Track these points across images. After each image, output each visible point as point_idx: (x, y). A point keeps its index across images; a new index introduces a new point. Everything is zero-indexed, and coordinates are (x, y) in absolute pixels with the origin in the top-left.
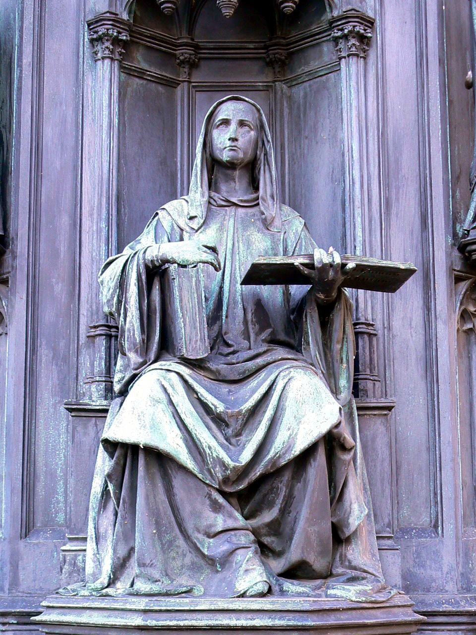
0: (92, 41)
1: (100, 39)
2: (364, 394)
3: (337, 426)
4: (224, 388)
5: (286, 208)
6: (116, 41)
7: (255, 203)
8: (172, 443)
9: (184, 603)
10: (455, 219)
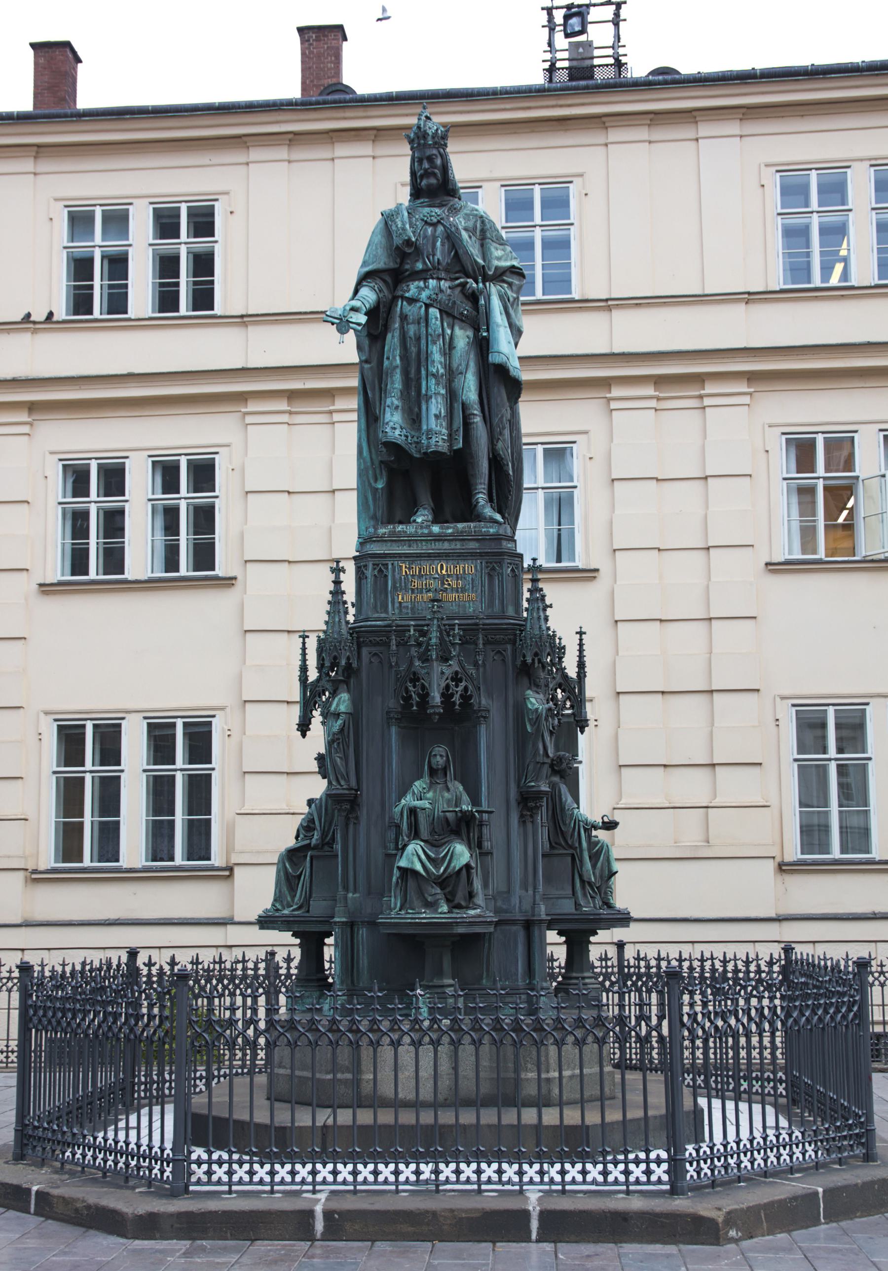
1: (391, 718)
4: (434, 849)
5: (456, 783)
6: (396, 719)
7: (446, 782)
8: (418, 867)
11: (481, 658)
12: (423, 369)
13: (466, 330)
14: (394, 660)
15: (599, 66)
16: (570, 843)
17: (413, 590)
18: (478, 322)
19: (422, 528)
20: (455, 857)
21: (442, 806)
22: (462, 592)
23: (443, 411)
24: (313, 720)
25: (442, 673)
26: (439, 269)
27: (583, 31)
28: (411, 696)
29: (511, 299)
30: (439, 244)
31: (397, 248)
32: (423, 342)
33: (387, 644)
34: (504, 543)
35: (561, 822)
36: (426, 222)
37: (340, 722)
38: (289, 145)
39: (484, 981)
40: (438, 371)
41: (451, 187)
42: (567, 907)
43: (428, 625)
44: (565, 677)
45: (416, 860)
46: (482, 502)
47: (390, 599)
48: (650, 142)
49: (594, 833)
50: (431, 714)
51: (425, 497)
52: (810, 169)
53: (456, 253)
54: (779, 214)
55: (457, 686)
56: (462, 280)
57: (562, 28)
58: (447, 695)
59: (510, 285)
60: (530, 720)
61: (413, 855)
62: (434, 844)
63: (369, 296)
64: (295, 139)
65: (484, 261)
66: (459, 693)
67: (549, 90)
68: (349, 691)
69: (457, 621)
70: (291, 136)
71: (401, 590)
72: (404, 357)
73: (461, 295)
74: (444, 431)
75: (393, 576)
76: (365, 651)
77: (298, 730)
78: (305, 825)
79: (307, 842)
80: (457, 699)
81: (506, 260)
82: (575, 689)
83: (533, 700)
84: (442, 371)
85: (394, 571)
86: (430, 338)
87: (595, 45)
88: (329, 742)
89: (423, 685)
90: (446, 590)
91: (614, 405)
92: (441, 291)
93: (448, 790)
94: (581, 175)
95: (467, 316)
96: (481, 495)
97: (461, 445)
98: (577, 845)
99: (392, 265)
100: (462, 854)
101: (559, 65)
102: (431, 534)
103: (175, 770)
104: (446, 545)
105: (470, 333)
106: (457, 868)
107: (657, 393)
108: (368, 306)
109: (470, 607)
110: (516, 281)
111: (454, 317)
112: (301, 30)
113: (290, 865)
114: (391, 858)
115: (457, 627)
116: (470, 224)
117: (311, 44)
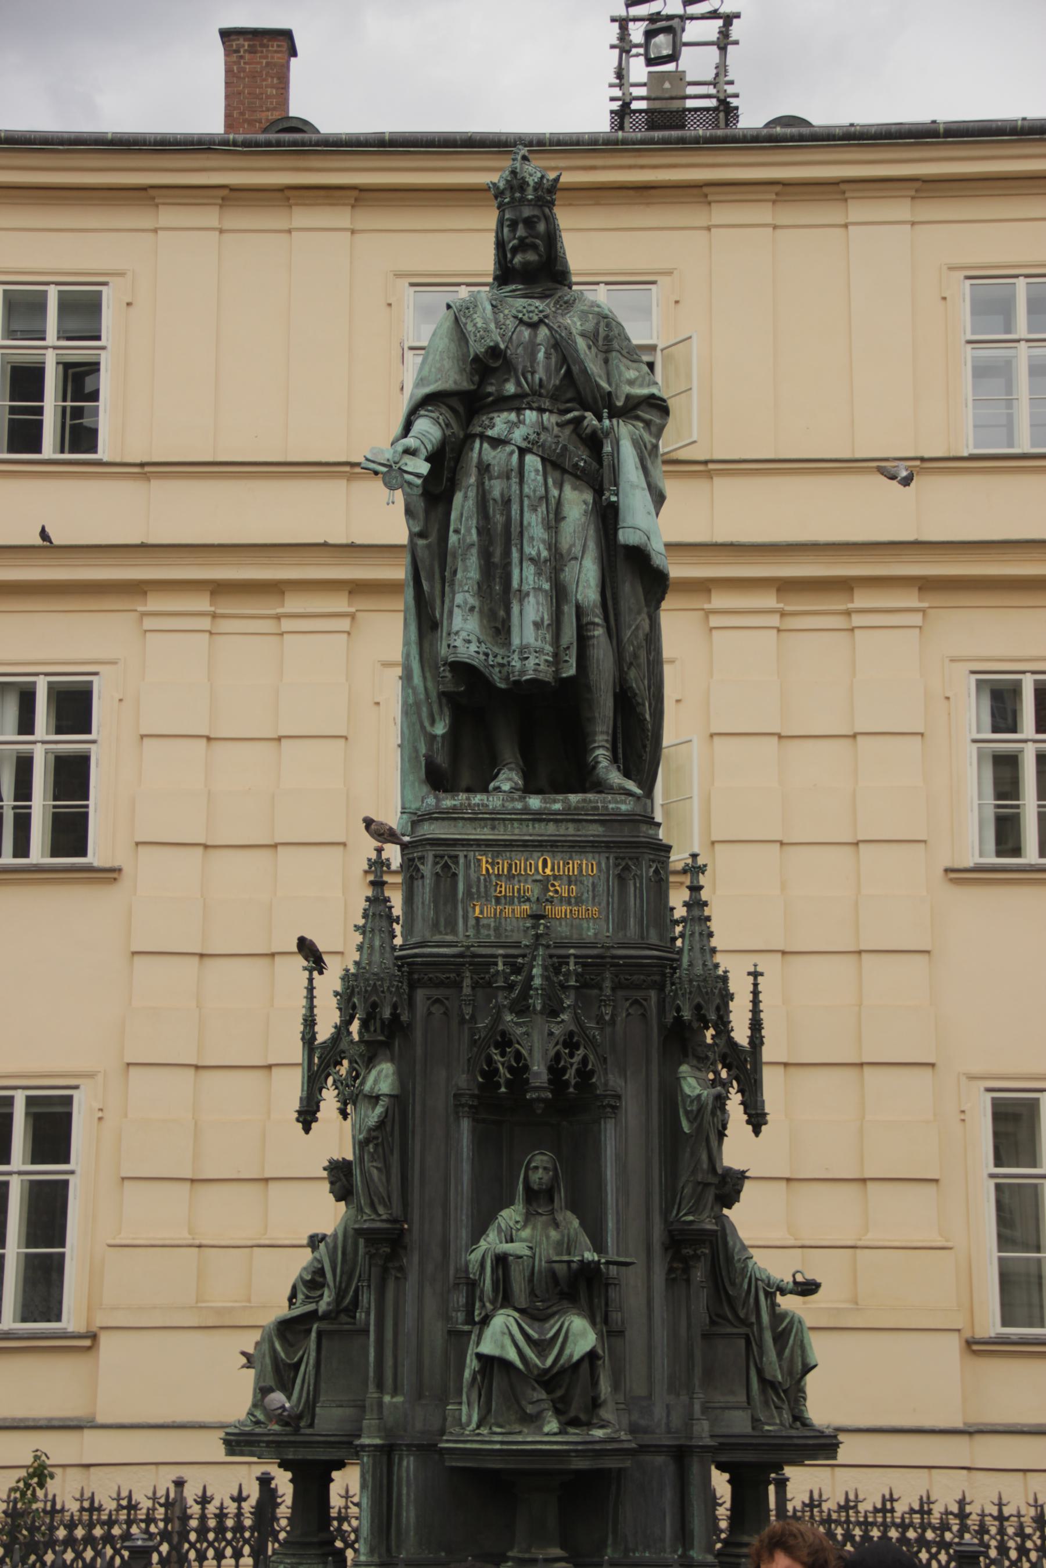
0: (456, 1106)
1: (463, 1105)
2: (610, 1330)
3: (594, 1347)
4: (536, 1325)
5: (569, 1214)
6: (471, 1107)
7: (552, 1212)
8: (512, 1355)
9: (520, 1438)
10: (665, 1213)
11: (609, 1010)
12: (514, 550)
13: (581, 491)
14: (468, 1011)
15: (696, 110)
16: (742, 1315)
17: (498, 900)
18: (599, 478)
19: (513, 800)
20: (571, 1339)
21: (547, 1252)
22: (577, 904)
23: (546, 617)
24: (322, 1104)
25: (551, 1034)
26: (541, 395)
27: (673, 57)
28: (497, 1070)
29: (649, 446)
30: (541, 355)
31: (476, 359)
32: (515, 508)
33: (458, 985)
34: (644, 828)
35: (726, 1280)
36: (521, 321)
37: (379, 1110)
38: (221, 206)
39: (609, 1551)
40: (539, 554)
41: (559, 268)
42: (739, 1423)
43: (524, 956)
44: (732, 1044)
45: (508, 1342)
46: (604, 763)
47: (461, 913)
48: (775, 227)
49: (779, 1299)
50: (532, 1100)
51: (508, 751)
52: (1017, 276)
53: (569, 371)
54: (969, 342)
55: (571, 1055)
56: (576, 413)
57: (641, 51)
58: (556, 1071)
59: (648, 424)
60: (687, 1113)
61: (503, 1333)
62: (533, 1314)
63: (428, 429)
64: (232, 196)
65: (610, 384)
66: (575, 1067)
67: (624, 142)
68: (392, 1060)
69: (572, 951)
70: (226, 192)
71: (479, 898)
72: (484, 530)
73: (574, 436)
74: (548, 648)
75: (467, 876)
76: (420, 994)
77: (298, 1120)
78: (308, 1277)
79: (311, 1307)
80: (570, 1075)
81: (641, 386)
82: (745, 1067)
83: (692, 1081)
84: (545, 554)
85: (467, 866)
86: (526, 502)
87: (689, 78)
88: (360, 1143)
89: (518, 1056)
90: (550, 901)
91: (715, 621)
92: (545, 428)
93: (557, 1226)
94: (669, 273)
95: (583, 470)
96: (601, 751)
97: (572, 671)
98: (753, 1319)
99: (465, 385)
100: (581, 1335)
101: (636, 105)
102: (526, 810)
103: (10, 1173)
104: (551, 829)
105: (589, 496)
106: (576, 1358)
107: (781, 605)
108: (429, 447)
109: (588, 929)
110: (654, 417)
111: (564, 471)
112: (226, 35)
113: (282, 1346)
114: (458, 1339)
115: (572, 961)
116: (589, 326)
117: (242, 57)
